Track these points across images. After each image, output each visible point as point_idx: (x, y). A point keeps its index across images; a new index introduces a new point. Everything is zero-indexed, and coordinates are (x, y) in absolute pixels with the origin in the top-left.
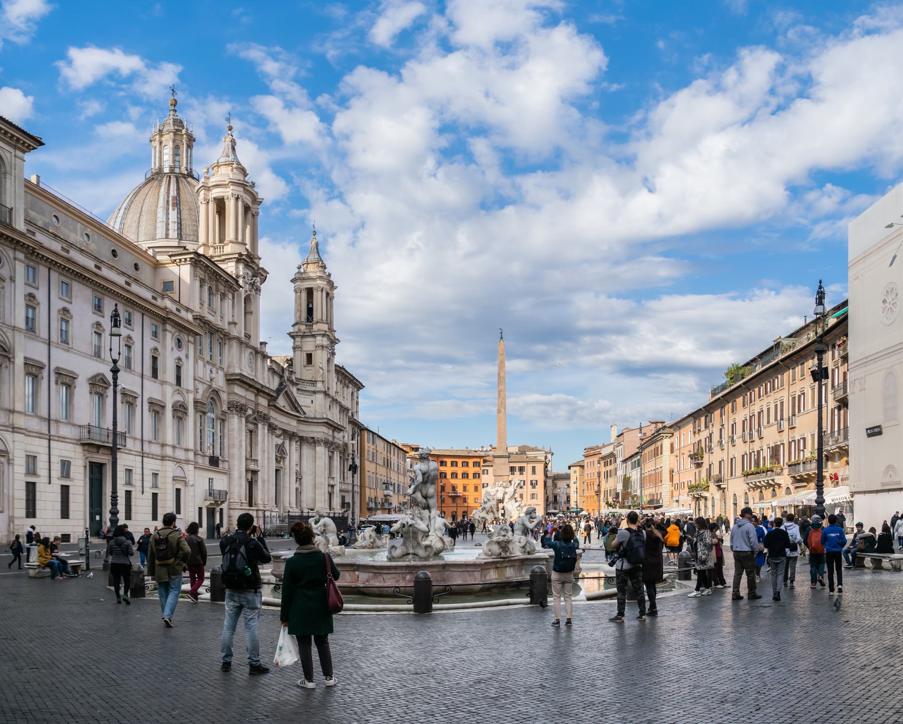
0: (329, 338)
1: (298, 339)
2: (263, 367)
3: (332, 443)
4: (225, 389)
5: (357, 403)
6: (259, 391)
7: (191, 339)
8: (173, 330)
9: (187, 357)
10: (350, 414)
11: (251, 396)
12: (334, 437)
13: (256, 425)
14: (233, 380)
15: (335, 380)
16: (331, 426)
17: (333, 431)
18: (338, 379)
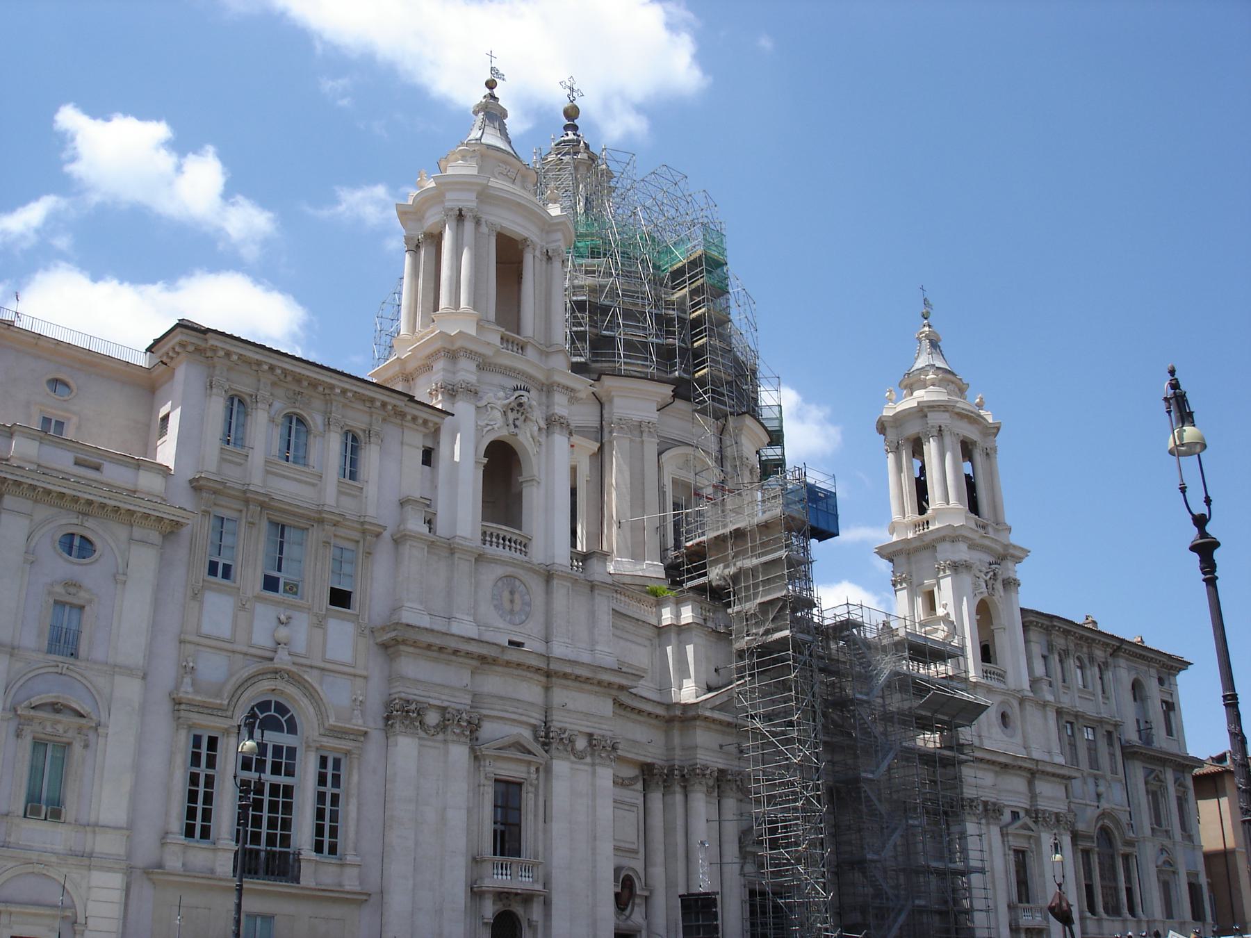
0: (973, 546)
1: (901, 560)
2: (592, 614)
3: (1036, 815)
4: (375, 667)
5: (1170, 707)
6: (549, 674)
7: (138, 533)
8: (42, 512)
9: (119, 578)
10: (1131, 735)
11: (530, 691)
12: (1033, 796)
13: (548, 770)
14: (393, 641)
15: (1037, 650)
16: (1005, 766)
17: (1031, 784)
18: (1050, 647)
